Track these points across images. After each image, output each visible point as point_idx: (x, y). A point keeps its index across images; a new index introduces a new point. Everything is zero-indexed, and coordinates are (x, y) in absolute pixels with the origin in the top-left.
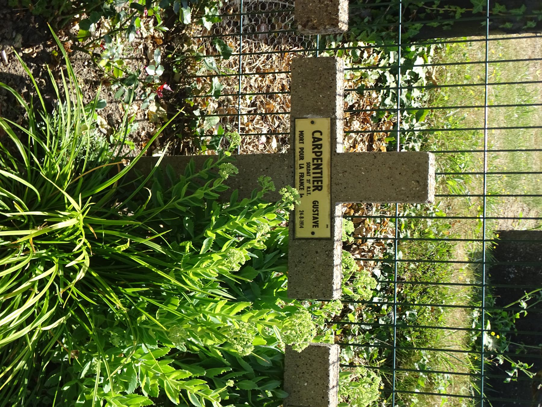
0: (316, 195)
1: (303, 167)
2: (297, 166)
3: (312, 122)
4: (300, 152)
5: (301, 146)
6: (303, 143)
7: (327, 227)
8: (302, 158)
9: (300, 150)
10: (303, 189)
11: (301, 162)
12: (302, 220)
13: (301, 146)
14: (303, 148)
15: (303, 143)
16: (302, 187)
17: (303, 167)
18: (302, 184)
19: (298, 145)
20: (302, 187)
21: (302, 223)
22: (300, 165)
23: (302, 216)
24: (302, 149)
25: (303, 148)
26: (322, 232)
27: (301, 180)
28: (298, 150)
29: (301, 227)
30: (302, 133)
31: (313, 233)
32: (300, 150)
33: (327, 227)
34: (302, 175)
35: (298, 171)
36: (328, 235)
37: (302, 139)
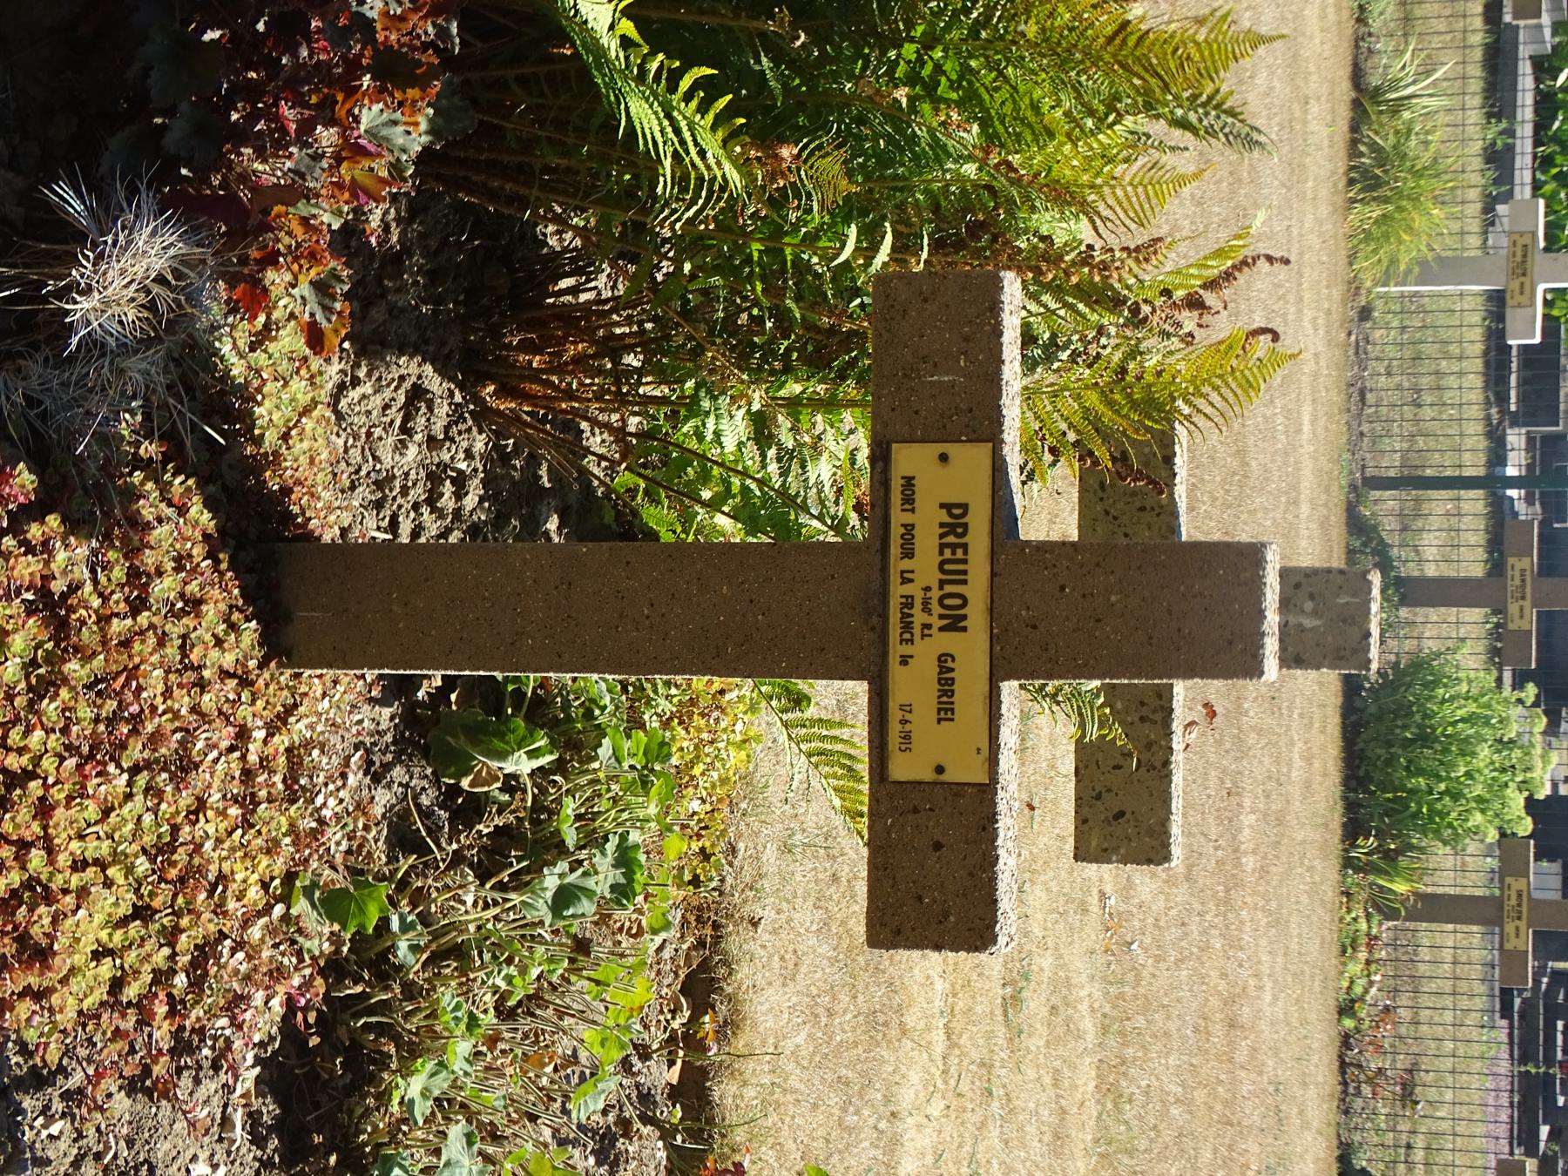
1: (912, 581)
2: (895, 578)
5: (907, 518)
6: (913, 510)
8: (908, 554)
9: (903, 530)
10: (912, 641)
11: (906, 564)
12: (908, 727)
13: (907, 518)
14: (913, 526)
15: (913, 510)
16: (907, 636)
17: (912, 581)
18: (907, 626)
19: (898, 517)
20: (907, 636)
21: (907, 737)
22: (903, 572)
23: (908, 717)
24: (909, 528)
25: (913, 526)
26: (966, 771)
27: (904, 615)
28: (896, 532)
30: (909, 482)
31: (940, 770)
32: (903, 530)
34: (908, 602)
35: (897, 591)
37: (909, 501)
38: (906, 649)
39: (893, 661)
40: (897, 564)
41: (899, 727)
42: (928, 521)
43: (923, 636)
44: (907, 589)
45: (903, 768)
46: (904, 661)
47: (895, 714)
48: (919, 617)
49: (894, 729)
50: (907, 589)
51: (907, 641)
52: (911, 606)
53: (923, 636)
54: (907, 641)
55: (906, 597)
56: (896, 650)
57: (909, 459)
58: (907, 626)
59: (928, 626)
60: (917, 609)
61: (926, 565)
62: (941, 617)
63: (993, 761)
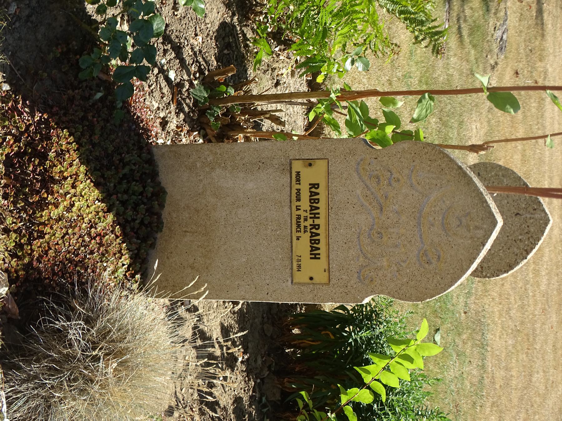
5: (298, 187)
6: (300, 184)
8: (298, 200)
9: (296, 191)
11: (298, 203)
12: (299, 263)
13: (298, 187)
15: (300, 184)
16: (299, 229)
18: (299, 226)
20: (299, 229)
21: (299, 266)
24: (299, 190)
27: (298, 222)
29: (298, 271)
30: (298, 173)
31: (311, 279)
32: (296, 191)
33: (325, 271)
34: (299, 217)
37: (298, 180)
38: (299, 234)
39: (294, 238)
44: (298, 213)
46: (298, 239)
47: (295, 259)
48: (303, 224)
50: (298, 213)
51: (299, 231)
54: (299, 231)
55: (298, 215)
58: (299, 226)
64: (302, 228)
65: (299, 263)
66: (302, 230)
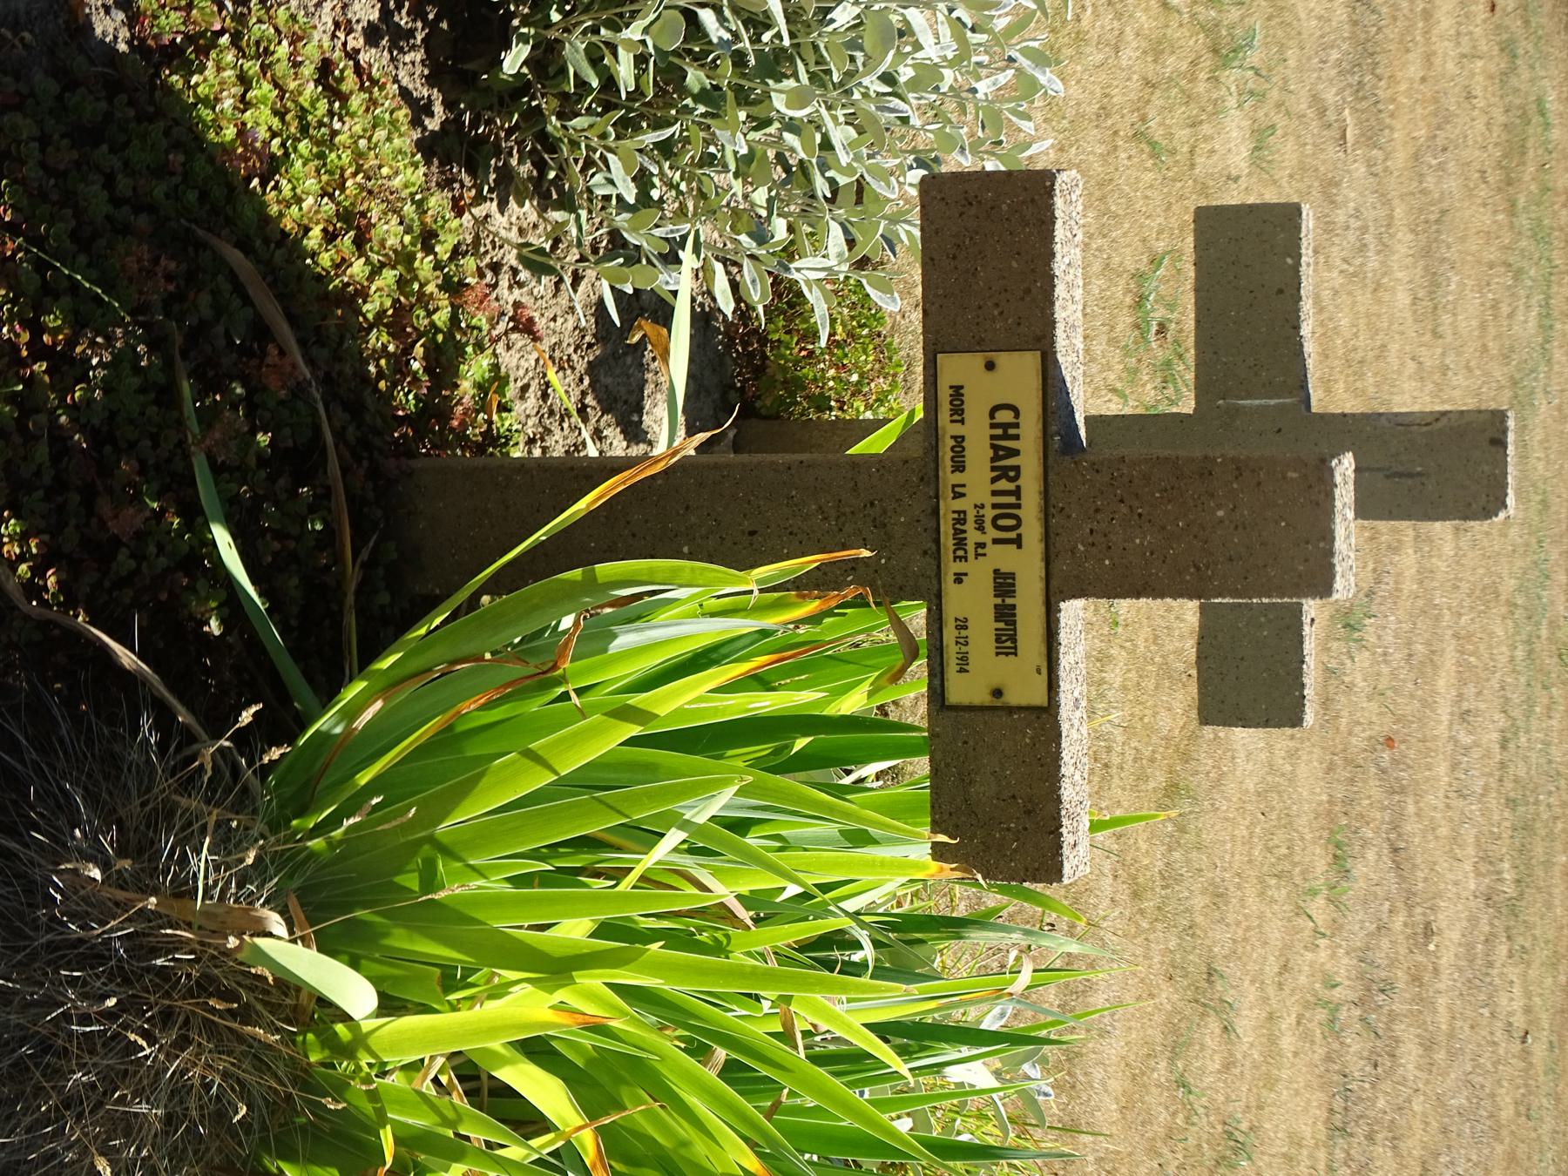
0: (1004, 557)
1: (963, 495)
3: (990, 366)
4: (952, 449)
5: (957, 429)
6: (962, 422)
7: (1039, 671)
8: (959, 467)
9: (952, 443)
11: (957, 478)
12: (964, 649)
13: (957, 429)
14: (963, 438)
15: (962, 422)
16: (960, 553)
17: (963, 495)
18: (960, 543)
19: (948, 428)
20: (960, 553)
21: (964, 659)
24: (960, 440)
25: (963, 438)
26: (1026, 691)
27: (957, 532)
29: (960, 671)
30: (957, 391)
31: (998, 693)
32: (952, 443)
33: (1039, 671)
34: (961, 518)
35: (948, 506)
36: (1040, 698)
37: (958, 412)
38: (959, 567)
40: (949, 478)
41: (957, 649)
42: (977, 434)
43: (977, 555)
44: (959, 504)
45: (960, 690)
46: (959, 578)
47: (950, 634)
48: (973, 536)
49: (951, 651)
50: (959, 504)
51: (960, 558)
52: (962, 521)
53: (977, 555)
54: (960, 558)
55: (959, 512)
56: (952, 568)
57: (954, 368)
58: (960, 543)
59: (982, 545)
60: (970, 525)
61: (978, 482)
62: (995, 506)
63: (1053, 686)
64: (971, 548)
65: (964, 649)
66: (971, 555)
